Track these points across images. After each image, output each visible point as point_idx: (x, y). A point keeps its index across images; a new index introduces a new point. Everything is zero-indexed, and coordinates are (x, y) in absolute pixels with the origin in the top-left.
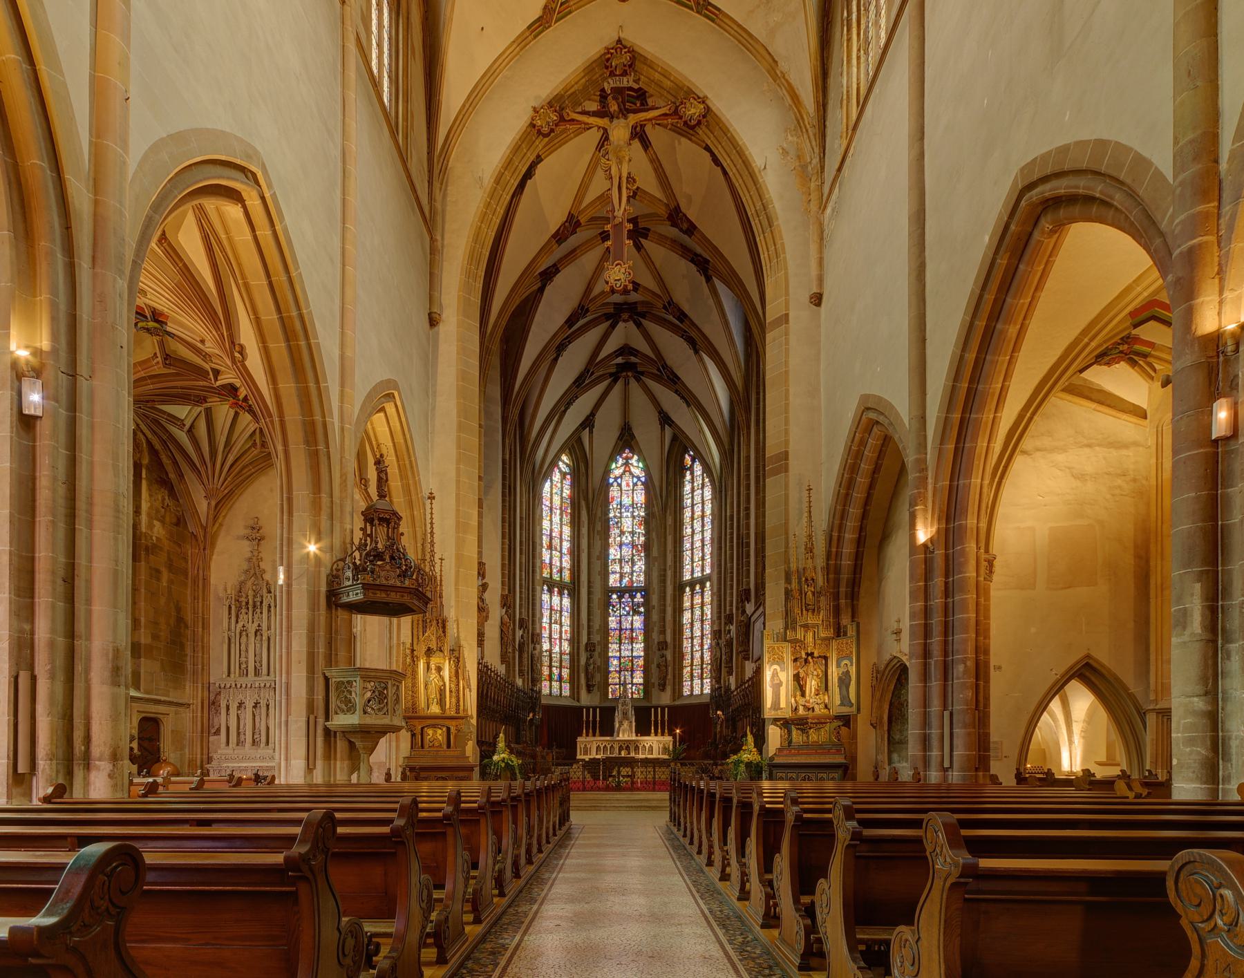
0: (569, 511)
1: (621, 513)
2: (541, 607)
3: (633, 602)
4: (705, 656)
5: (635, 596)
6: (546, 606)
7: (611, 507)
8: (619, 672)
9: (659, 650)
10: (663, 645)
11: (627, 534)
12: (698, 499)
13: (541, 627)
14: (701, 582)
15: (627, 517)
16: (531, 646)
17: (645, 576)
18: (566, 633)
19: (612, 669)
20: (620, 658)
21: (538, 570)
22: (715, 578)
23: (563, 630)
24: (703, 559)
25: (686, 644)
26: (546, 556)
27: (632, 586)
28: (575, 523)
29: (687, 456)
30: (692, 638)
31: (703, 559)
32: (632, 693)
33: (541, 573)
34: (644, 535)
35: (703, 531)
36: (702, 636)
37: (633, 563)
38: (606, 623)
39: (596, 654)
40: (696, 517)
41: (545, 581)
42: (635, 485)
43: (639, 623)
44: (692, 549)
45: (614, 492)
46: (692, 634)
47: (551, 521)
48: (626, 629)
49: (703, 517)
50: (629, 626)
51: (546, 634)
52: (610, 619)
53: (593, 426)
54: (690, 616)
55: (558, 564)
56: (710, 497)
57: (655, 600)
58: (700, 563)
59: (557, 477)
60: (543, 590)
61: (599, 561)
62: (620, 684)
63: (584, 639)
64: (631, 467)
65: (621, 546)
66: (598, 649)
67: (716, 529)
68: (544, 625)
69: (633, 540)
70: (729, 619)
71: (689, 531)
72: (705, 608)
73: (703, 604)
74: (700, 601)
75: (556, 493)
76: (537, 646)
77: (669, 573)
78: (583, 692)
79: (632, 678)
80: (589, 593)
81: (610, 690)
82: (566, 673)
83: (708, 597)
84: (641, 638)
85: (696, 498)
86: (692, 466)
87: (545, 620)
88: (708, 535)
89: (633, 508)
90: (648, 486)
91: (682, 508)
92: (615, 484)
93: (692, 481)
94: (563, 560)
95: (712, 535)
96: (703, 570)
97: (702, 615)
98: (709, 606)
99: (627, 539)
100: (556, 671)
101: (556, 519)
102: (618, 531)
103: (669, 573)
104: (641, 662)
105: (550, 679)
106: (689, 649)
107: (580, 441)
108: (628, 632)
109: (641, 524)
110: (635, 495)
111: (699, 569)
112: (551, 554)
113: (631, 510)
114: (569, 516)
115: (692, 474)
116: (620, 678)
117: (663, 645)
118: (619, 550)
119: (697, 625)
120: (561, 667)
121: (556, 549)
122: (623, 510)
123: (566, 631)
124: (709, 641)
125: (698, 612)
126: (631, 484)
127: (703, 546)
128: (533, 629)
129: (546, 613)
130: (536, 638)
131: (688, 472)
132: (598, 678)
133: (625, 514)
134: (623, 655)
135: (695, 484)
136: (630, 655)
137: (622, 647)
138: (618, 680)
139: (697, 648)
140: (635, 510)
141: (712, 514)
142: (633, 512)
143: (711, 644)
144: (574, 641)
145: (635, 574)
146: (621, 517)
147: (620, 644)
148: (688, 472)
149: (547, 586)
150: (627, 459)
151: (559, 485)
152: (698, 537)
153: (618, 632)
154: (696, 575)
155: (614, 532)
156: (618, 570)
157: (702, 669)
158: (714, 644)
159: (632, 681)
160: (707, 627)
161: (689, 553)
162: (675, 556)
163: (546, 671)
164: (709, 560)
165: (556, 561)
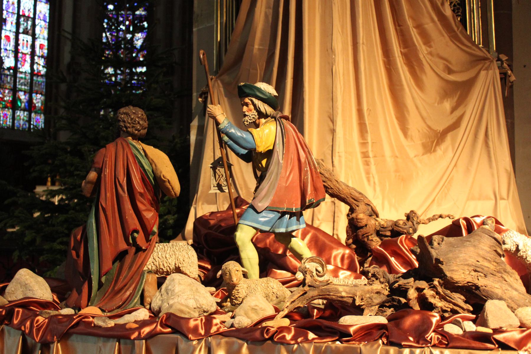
18: (41, 47)
23: (37, 43)
82: (38, 100)
100: (22, 96)
120: (30, 92)
129: (11, 20)
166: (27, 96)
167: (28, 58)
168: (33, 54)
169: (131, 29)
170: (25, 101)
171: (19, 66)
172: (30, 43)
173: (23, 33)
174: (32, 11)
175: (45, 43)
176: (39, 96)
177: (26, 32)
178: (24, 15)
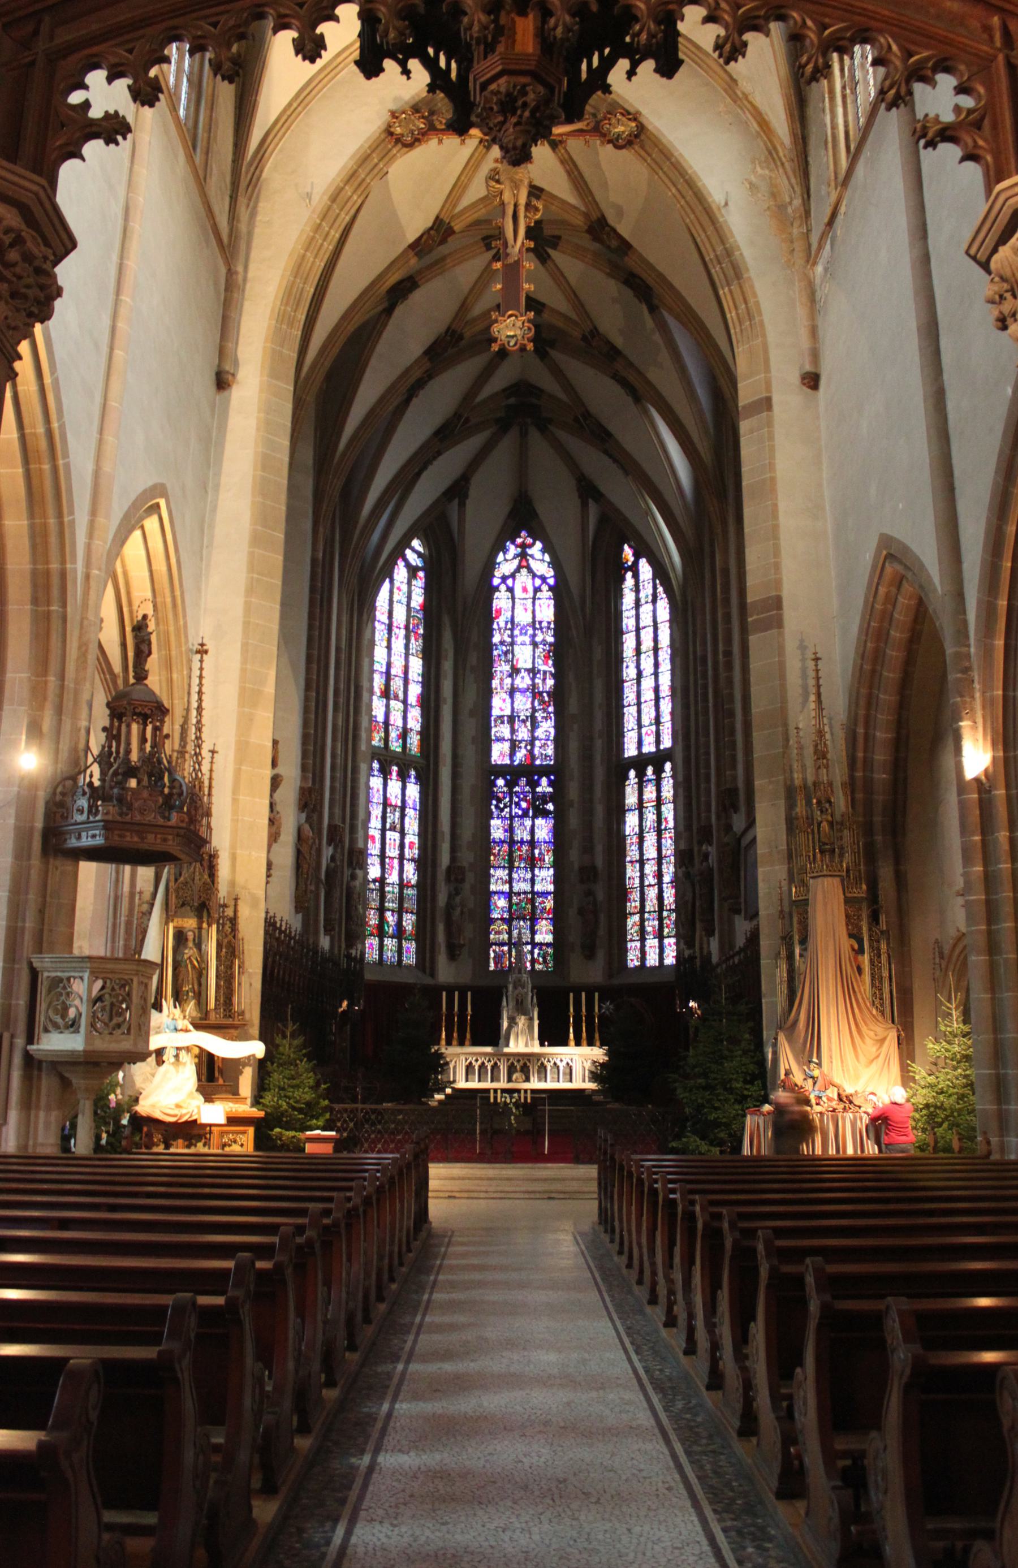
0: (421, 631)
1: (512, 636)
2: (368, 801)
3: (534, 792)
4: (665, 895)
5: (538, 784)
6: (377, 797)
7: (495, 626)
8: (508, 922)
9: (582, 881)
10: (588, 873)
11: (523, 673)
12: (646, 619)
13: (367, 837)
14: (658, 759)
15: (523, 644)
16: (347, 873)
17: (556, 748)
18: (411, 847)
19: (495, 915)
20: (509, 896)
21: (363, 735)
22: (679, 756)
23: (407, 841)
24: (658, 721)
25: (632, 872)
27: (532, 764)
28: (430, 656)
30: (642, 862)
31: (658, 721)
32: (533, 961)
33: (370, 739)
34: (554, 676)
35: (656, 674)
38: (487, 829)
39: (467, 886)
40: (643, 648)
42: (537, 590)
44: (639, 704)
45: (501, 600)
46: (641, 854)
47: (389, 647)
48: (522, 842)
49: (656, 650)
50: (527, 837)
51: (374, 849)
52: (493, 822)
54: (637, 823)
55: (400, 723)
56: (667, 617)
57: (573, 791)
58: (653, 728)
59: (401, 573)
60: (372, 769)
62: (509, 943)
63: (445, 859)
64: (531, 561)
65: (512, 692)
66: (470, 878)
68: (371, 832)
69: (534, 685)
70: (705, 835)
72: (663, 808)
73: (659, 802)
74: (654, 795)
75: (399, 602)
76: (359, 873)
77: (599, 743)
78: (442, 959)
79: (533, 933)
80: (455, 775)
81: (492, 955)
82: (409, 921)
84: (549, 858)
85: (642, 616)
86: (636, 563)
87: (375, 823)
88: (665, 680)
89: (535, 629)
91: (620, 632)
92: (503, 587)
93: (637, 589)
95: (672, 680)
96: (658, 742)
97: (659, 821)
98: (671, 806)
99: (523, 681)
100: (391, 918)
101: (398, 645)
103: (599, 743)
104: (549, 904)
105: (381, 932)
106: (637, 881)
108: (525, 848)
109: (547, 657)
111: (652, 739)
112: (387, 706)
113: (530, 631)
114: (420, 641)
115: (636, 576)
116: (510, 933)
117: (588, 873)
118: (508, 700)
119: (650, 839)
120: (400, 911)
121: (396, 698)
122: (516, 632)
123: (412, 844)
124: (672, 869)
125: (650, 817)
127: (657, 699)
128: (353, 841)
129: (376, 812)
130: (358, 858)
131: (629, 575)
132: (469, 932)
133: (519, 639)
134: (516, 889)
135: (642, 595)
136: (528, 888)
137: (515, 876)
138: (506, 937)
139: (651, 880)
140: (538, 632)
141: (672, 645)
142: (534, 636)
143: (675, 873)
144: (425, 863)
145: (538, 743)
146: (512, 644)
147: (511, 869)
148: (629, 575)
149: (379, 762)
150: (524, 546)
151: (405, 588)
152: (648, 683)
153: (506, 847)
155: (502, 668)
156: (507, 734)
158: (680, 875)
159: (533, 938)
161: (633, 710)
162: (609, 715)
164: (669, 725)
165: (396, 719)
166: (396, 916)
167: (396, 862)
169: (531, 814)
170: (393, 923)
172: (398, 842)
174: (400, 796)
175: (415, 840)
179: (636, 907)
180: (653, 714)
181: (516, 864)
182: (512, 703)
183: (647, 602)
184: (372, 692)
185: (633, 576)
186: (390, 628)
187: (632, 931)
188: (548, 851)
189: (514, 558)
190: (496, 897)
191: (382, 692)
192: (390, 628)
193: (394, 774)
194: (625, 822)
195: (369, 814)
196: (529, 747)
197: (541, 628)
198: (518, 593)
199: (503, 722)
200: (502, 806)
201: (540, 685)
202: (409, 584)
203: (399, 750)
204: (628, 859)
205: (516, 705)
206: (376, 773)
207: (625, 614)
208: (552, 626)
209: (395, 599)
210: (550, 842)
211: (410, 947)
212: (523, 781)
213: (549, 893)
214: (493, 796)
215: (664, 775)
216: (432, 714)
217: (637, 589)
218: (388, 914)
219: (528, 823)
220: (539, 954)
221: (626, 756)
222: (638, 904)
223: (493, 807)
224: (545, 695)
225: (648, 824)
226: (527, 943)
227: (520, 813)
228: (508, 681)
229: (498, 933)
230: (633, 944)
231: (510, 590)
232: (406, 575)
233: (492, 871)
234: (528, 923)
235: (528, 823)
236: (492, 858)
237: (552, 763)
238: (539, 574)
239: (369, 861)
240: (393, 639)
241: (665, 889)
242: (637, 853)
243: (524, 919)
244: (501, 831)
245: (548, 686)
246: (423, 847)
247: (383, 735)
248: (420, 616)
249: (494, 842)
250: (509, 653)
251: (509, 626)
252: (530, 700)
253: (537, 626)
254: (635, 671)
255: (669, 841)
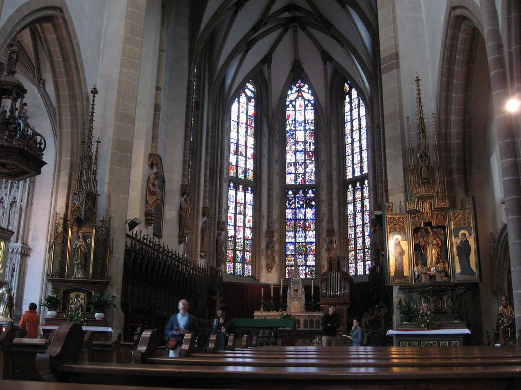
0: (253, 125)
1: (295, 127)
3: (306, 197)
6: (232, 199)
7: (287, 123)
11: (300, 143)
14: (362, 179)
15: (300, 130)
18: (249, 222)
19: (288, 253)
20: (295, 244)
21: (225, 170)
23: (247, 219)
24: (361, 162)
25: (351, 232)
26: (233, 159)
27: (305, 184)
28: (258, 136)
29: (346, 84)
30: (355, 226)
31: (361, 162)
33: (228, 173)
34: (314, 144)
36: (363, 225)
37: (306, 167)
40: (354, 129)
41: (231, 179)
42: (306, 106)
43: (311, 214)
45: (290, 111)
47: (238, 132)
48: (300, 219)
50: (302, 217)
52: (287, 211)
53: (271, 62)
57: (324, 195)
58: (359, 165)
59: (243, 99)
60: (230, 186)
61: (277, 164)
64: (303, 93)
65: (295, 152)
67: (370, 139)
68: (229, 215)
69: (305, 148)
71: (349, 140)
73: (363, 198)
74: (360, 196)
75: (243, 112)
76: (223, 233)
77: (335, 173)
79: (306, 261)
81: (287, 271)
82: (248, 256)
83: (366, 194)
84: (313, 227)
87: (231, 211)
89: (305, 123)
90: (316, 107)
91: (344, 123)
92: (291, 106)
93: (351, 103)
94: (247, 163)
98: (368, 200)
99: (300, 147)
101: (242, 131)
102: (293, 141)
103: (335, 173)
104: (313, 247)
105: (234, 260)
106: (353, 235)
107: (261, 72)
108: (302, 222)
109: (311, 136)
110: (306, 114)
112: (237, 158)
113: (303, 125)
114: (253, 130)
115: (350, 97)
118: (294, 156)
119: (359, 216)
120: (244, 251)
121: (241, 155)
122: (297, 125)
125: (359, 206)
126: (303, 106)
130: (223, 226)
131: (347, 96)
133: (298, 128)
134: (298, 241)
135: (353, 105)
136: (304, 241)
137: (297, 235)
138: (293, 263)
139: (359, 235)
140: (307, 125)
142: (305, 126)
144: (255, 229)
145: (307, 175)
146: (295, 130)
147: (295, 231)
148: (347, 96)
149: (234, 184)
150: (300, 87)
151: (245, 106)
152: (356, 145)
153: (293, 222)
154: (356, 175)
155: (291, 141)
156: (293, 171)
157: (364, 253)
159: (306, 263)
160: (367, 217)
161: (350, 157)
162: (339, 160)
163: (230, 254)
165: (242, 164)
166: (242, 253)
167: (242, 229)
168: (244, 227)
170: (240, 256)
171: (237, 235)
172: (242, 220)
173: (239, 214)
174: (243, 199)
175: (251, 219)
176: (248, 253)
177: (240, 213)
178: (239, 203)
179: (353, 248)
180: (359, 159)
181: (298, 230)
182: (295, 157)
183: (355, 108)
184: (229, 152)
185: (349, 97)
186: (238, 123)
187: (351, 259)
188: (312, 223)
189: (296, 92)
190: (289, 245)
191: (235, 152)
192: (238, 123)
193: (241, 189)
194: (347, 209)
195: (228, 207)
196: (303, 177)
197: (308, 123)
198: (298, 108)
199: (291, 166)
200: (291, 203)
201: (308, 149)
202: (247, 104)
203: (243, 178)
204: (349, 225)
205: (297, 158)
206: (232, 188)
207: (346, 114)
208: (313, 122)
209: (240, 111)
210: (313, 219)
211: (248, 268)
212: (301, 192)
213: (313, 243)
214: (287, 199)
215: (364, 186)
216: (258, 162)
217: (351, 103)
218: (238, 252)
219: (303, 211)
220: (309, 270)
221: (347, 178)
222: (353, 246)
223: (287, 204)
224: (310, 153)
225: (358, 209)
226: (303, 266)
227: (299, 206)
228: (293, 147)
229: (290, 261)
230: (352, 265)
231: (294, 106)
232: (246, 100)
233: (287, 233)
234: (304, 256)
235: (303, 211)
236: (287, 227)
237: (314, 183)
238: (307, 99)
239: (228, 228)
240: (240, 129)
241: (366, 239)
242: (353, 223)
243: (302, 255)
244: (291, 214)
245: (312, 149)
246: (254, 222)
247: (235, 171)
248: (253, 119)
249: (288, 220)
250: (293, 135)
251: (294, 122)
252: (303, 155)
253: (307, 122)
254: (351, 139)
255: (368, 216)
